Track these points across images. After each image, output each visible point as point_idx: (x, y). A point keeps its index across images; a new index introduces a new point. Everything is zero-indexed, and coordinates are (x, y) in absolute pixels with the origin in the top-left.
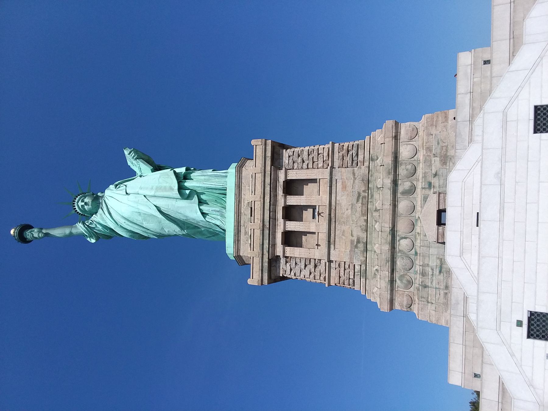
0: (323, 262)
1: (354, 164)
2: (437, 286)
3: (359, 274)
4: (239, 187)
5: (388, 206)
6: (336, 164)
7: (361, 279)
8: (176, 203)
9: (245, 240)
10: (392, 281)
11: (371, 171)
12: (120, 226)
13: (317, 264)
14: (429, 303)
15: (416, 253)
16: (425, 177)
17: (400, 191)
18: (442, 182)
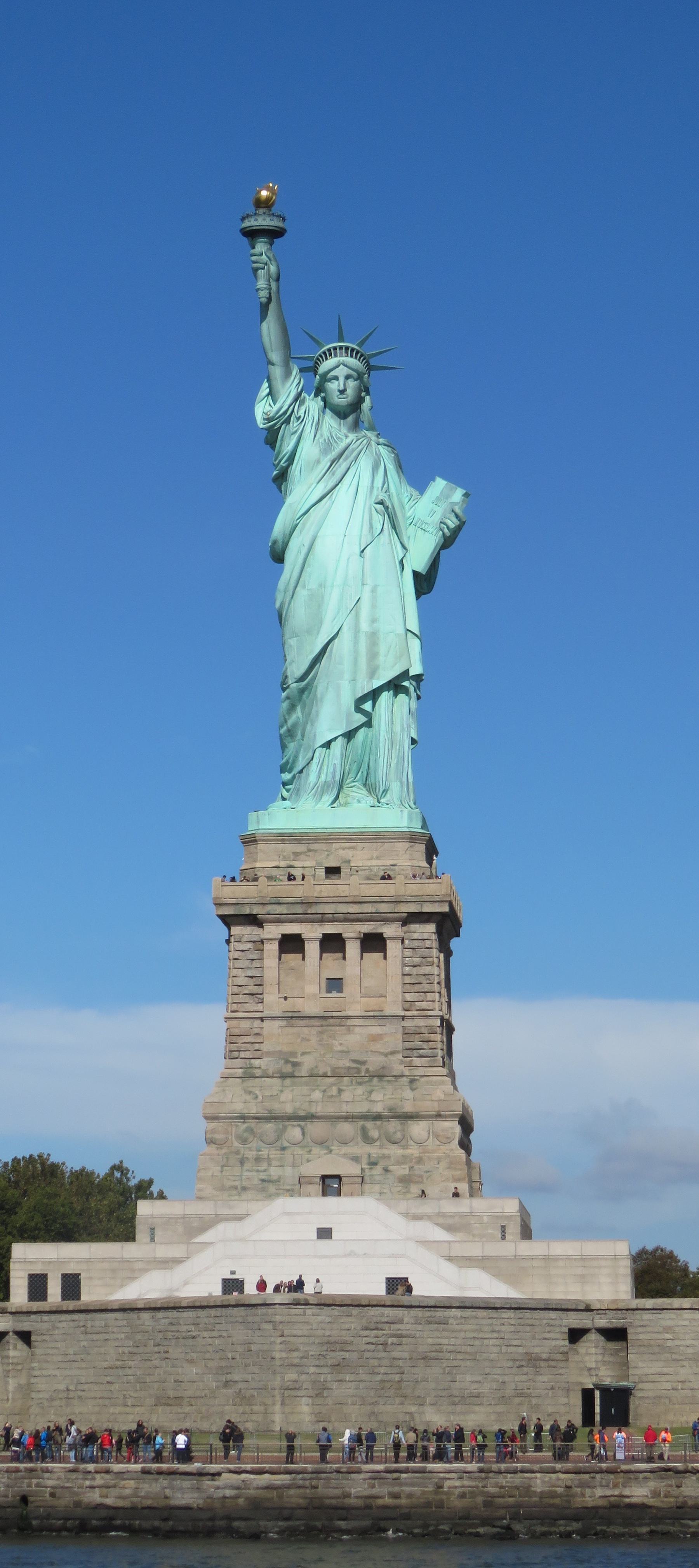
0: (259, 1007)
1: (407, 1053)
2: (244, 1177)
3: (246, 1065)
4: (375, 839)
5: (346, 1109)
6: (407, 1023)
7: (240, 1070)
8: (347, 682)
9: (284, 854)
10: (243, 1118)
11: (396, 1081)
12: (297, 525)
13: (256, 997)
14: (222, 1169)
15: (284, 1149)
16: (384, 1157)
17: (366, 1125)
18: (377, 1178)
